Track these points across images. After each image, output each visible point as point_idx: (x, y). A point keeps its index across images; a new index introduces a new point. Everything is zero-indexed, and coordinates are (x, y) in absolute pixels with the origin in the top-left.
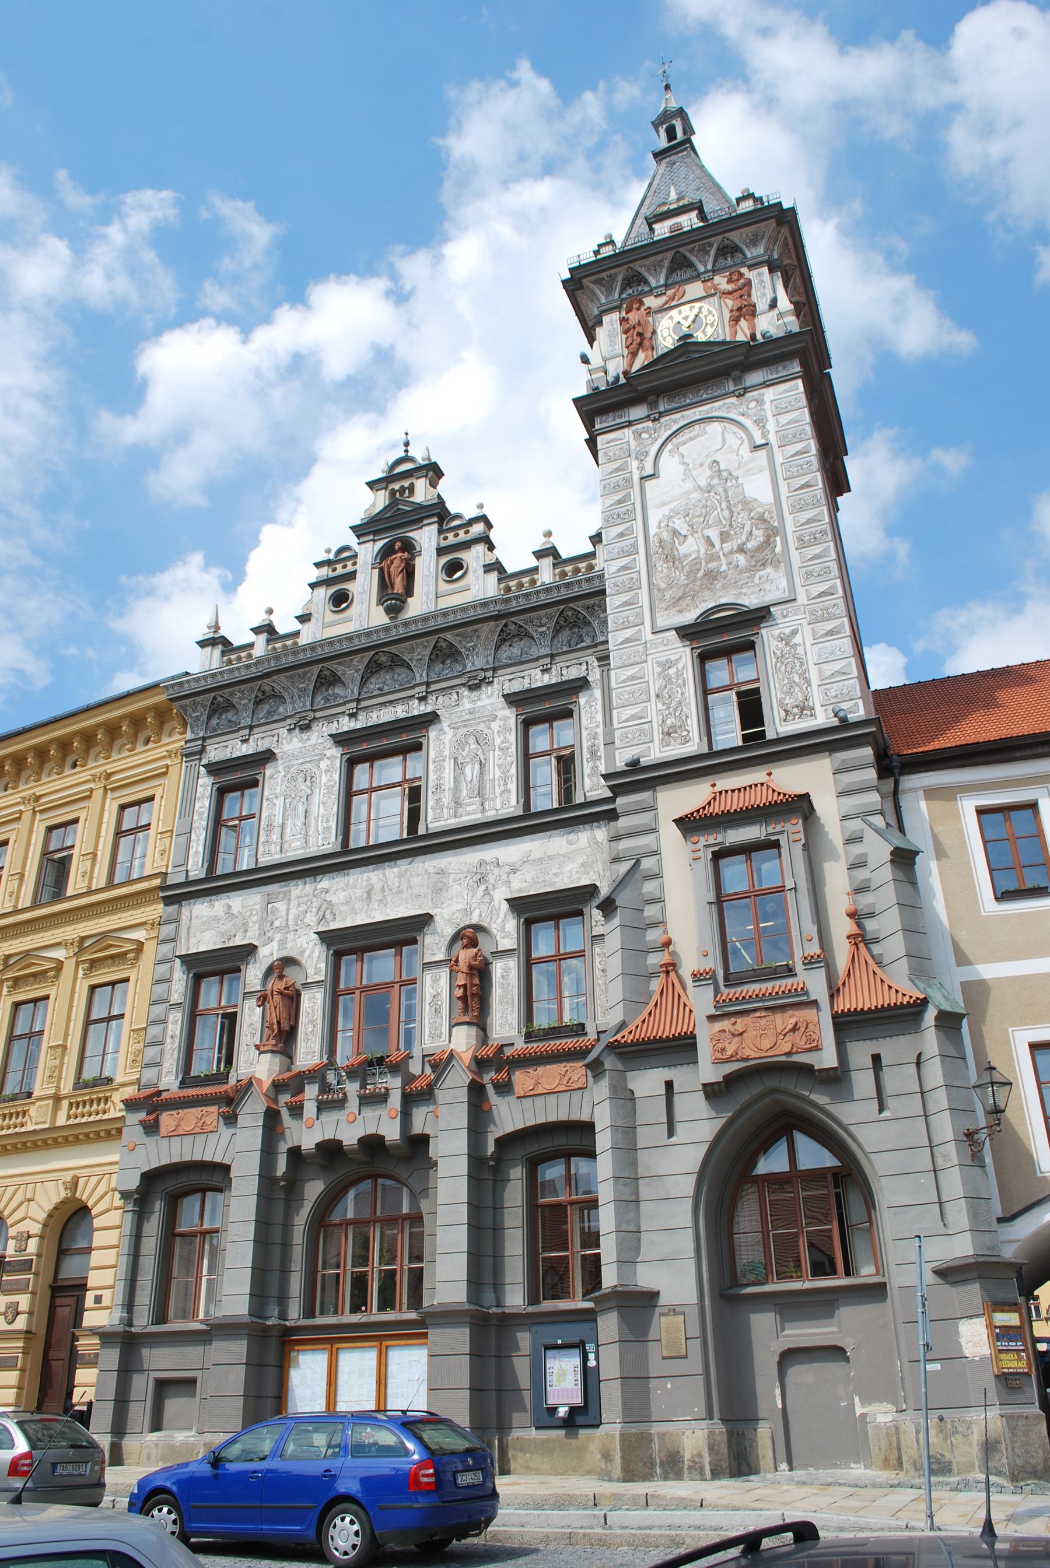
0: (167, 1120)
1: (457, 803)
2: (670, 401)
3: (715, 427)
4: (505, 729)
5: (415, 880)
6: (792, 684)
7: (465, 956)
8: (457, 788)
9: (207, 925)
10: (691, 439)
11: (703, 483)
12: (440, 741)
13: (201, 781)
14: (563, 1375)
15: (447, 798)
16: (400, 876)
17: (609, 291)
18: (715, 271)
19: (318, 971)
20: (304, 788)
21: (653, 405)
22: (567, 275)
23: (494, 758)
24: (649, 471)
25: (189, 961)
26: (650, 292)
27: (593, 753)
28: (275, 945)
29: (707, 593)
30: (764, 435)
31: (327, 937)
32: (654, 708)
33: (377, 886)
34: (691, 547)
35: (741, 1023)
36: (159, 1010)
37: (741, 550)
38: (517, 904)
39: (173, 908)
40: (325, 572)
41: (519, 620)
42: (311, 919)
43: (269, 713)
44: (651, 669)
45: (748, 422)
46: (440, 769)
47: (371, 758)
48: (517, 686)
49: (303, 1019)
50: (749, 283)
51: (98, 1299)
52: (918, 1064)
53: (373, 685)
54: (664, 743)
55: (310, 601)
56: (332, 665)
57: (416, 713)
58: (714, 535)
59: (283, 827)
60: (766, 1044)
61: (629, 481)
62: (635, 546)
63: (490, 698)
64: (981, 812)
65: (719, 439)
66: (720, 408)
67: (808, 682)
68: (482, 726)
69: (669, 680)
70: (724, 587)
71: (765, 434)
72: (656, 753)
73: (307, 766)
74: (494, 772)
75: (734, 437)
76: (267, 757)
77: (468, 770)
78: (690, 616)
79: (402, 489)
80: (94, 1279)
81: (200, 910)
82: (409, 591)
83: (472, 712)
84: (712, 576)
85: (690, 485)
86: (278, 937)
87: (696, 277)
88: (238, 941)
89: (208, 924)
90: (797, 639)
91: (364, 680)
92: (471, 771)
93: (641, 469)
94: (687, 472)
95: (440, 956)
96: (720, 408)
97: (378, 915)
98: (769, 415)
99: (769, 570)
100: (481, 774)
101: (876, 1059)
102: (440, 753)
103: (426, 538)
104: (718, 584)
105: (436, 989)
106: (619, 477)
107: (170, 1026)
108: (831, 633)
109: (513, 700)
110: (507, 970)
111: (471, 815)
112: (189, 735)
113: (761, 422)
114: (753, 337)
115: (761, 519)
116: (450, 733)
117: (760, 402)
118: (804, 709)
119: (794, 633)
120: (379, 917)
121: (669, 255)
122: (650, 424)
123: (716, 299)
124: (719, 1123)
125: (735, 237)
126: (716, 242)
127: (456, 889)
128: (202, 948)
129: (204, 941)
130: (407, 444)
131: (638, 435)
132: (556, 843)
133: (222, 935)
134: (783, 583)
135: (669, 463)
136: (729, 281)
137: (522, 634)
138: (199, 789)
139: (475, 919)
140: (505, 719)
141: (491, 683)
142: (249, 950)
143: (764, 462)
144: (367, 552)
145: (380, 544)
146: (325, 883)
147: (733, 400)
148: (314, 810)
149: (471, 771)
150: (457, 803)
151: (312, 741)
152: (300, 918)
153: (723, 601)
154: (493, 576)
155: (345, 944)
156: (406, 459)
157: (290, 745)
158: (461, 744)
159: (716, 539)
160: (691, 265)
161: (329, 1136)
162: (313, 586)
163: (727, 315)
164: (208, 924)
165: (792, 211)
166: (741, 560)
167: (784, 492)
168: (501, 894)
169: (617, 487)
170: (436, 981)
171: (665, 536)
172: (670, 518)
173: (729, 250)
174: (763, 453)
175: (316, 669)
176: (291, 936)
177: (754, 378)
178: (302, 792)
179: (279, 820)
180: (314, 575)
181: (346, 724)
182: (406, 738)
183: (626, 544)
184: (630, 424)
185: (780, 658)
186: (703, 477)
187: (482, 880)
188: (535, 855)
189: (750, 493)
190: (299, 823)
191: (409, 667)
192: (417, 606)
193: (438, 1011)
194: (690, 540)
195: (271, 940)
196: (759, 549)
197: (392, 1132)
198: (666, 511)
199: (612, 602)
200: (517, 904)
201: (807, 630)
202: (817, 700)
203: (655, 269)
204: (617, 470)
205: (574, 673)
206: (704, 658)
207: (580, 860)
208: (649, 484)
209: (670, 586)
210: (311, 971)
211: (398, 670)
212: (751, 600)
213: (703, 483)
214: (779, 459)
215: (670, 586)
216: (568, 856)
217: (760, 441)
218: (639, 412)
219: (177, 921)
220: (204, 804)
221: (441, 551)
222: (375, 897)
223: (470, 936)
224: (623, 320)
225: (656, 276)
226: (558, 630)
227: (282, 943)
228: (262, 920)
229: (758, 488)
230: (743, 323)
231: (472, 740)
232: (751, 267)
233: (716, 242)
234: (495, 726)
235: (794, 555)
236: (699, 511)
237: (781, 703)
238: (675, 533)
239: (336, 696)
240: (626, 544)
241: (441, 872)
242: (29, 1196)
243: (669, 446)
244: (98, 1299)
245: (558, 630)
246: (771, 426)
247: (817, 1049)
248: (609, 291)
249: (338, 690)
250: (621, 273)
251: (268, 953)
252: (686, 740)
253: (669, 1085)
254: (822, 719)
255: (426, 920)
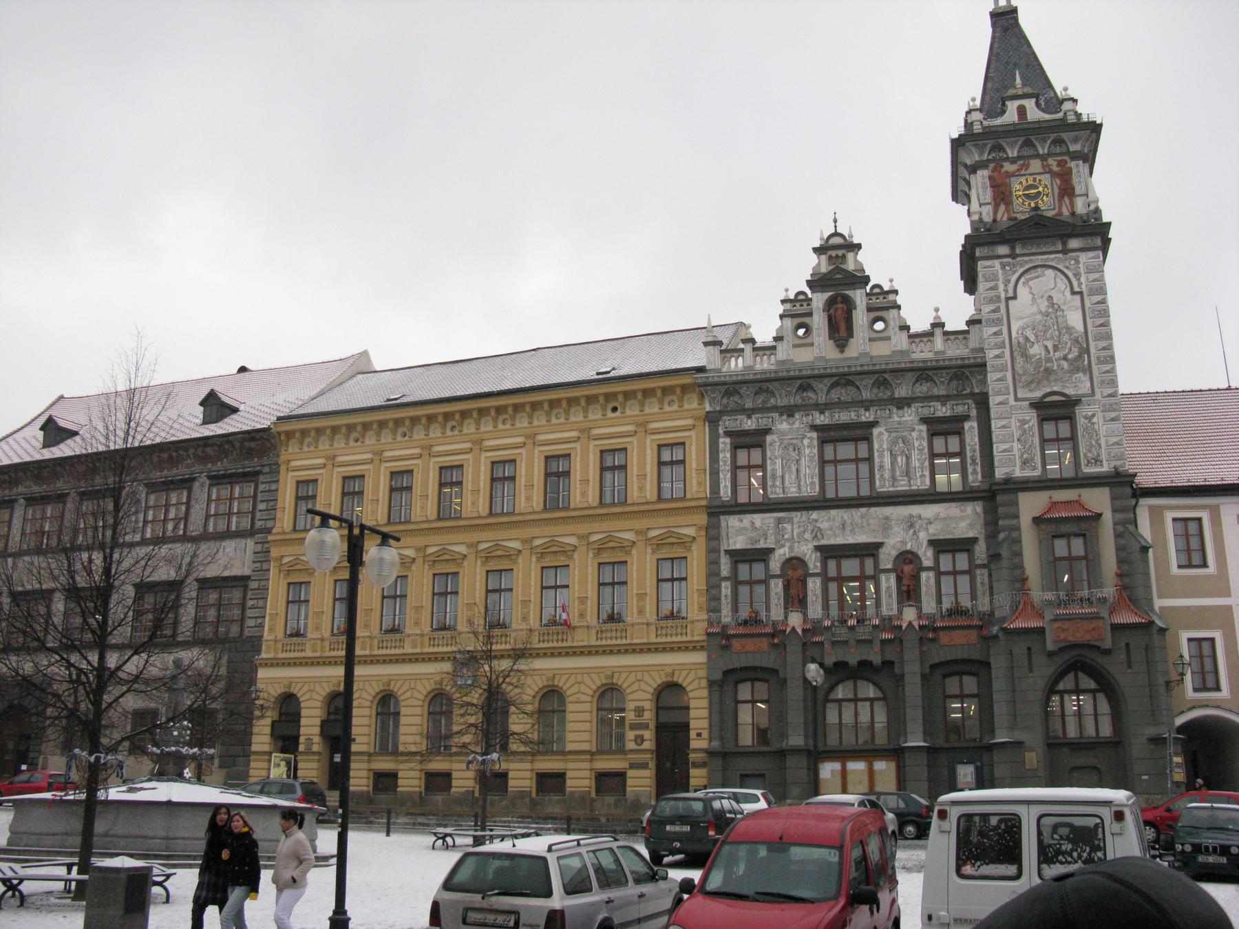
0: (736, 644)
1: (894, 478)
2: (1023, 247)
3: (1050, 272)
4: (920, 438)
5: (871, 521)
6: (1091, 446)
7: (908, 569)
8: (893, 470)
9: (739, 532)
10: (1036, 277)
11: (1043, 310)
12: (881, 438)
13: (721, 440)
14: (965, 775)
15: (887, 475)
16: (862, 517)
17: (982, 153)
18: (1050, 155)
19: (816, 567)
20: (794, 455)
21: (1013, 248)
22: (956, 136)
23: (915, 455)
24: (1011, 294)
25: (732, 553)
26: (1007, 159)
27: (974, 461)
28: (786, 549)
29: (1045, 382)
30: (1080, 284)
31: (817, 548)
32: (1016, 446)
33: (849, 522)
34: (1036, 350)
35: (1066, 625)
36: (713, 580)
37: (1065, 358)
38: (932, 543)
39: (713, 520)
40: (788, 306)
41: (930, 373)
42: (807, 536)
43: (764, 402)
44: (1014, 423)
45: (1070, 274)
46: (881, 456)
47: (834, 441)
48: (926, 412)
49: (809, 593)
50: (1070, 171)
51: (699, 735)
52: (1146, 648)
53: (834, 395)
54: (1022, 468)
55: (781, 327)
56: (812, 382)
57: (863, 419)
58: (1050, 345)
59: (783, 477)
60: (1079, 635)
61: (999, 297)
62: (1003, 342)
63: (909, 416)
64: (1174, 520)
65: (1052, 281)
66: (1052, 260)
67: (1100, 446)
68: (905, 434)
69: (1025, 431)
70: (1055, 380)
71: (1080, 284)
72: (1018, 473)
73: (795, 441)
74: (915, 463)
75: (1062, 284)
76: (767, 431)
77: (899, 459)
78: (1038, 394)
79: (837, 256)
80: (693, 724)
81: (732, 523)
82: (851, 335)
83: (899, 423)
84: (1048, 371)
85: (1035, 309)
86: (788, 544)
87: (1037, 156)
88: (762, 545)
89: (741, 531)
90: (1095, 420)
91: (828, 392)
92: (901, 460)
93: (1006, 291)
94: (1034, 299)
95: (889, 566)
96: (1052, 260)
97: (851, 540)
98: (1082, 271)
99: (1081, 374)
100: (908, 463)
101: (1127, 645)
102: (881, 446)
103: (859, 297)
104: (1052, 378)
105: (889, 582)
106: (993, 293)
107: (724, 591)
108: (1113, 420)
109: (924, 420)
110: (928, 578)
111: (902, 486)
112: (708, 408)
113: (1077, 275)
114: (1073, 214)
115: (1077, 341)
116: (886, 435)
117: (1077, 262)
118: (1097, 461)
119: (1093, 416)
120: (851, 540)
121: (1023, 139)
122: (1009, 260)
123: (1048, 176)
124: (1053, 670)
125: (1065, 136)
126: (1053, 136)
127: (896, 529)
128: (738, 547)
129: (739, 543)
130: (835, 221)
131: (1003, 266)
132: (952, 509)
133: (751, 539)
134: (1089, 385)
135: (1022, 291)
136: (1058, 165)
137: (929, 379)
138: (721, 446)
139: (909, 547)
140: (921, 431)
141: (909, 406)
142: (770, 551)
143: (1078, 303)
144: (819, 300)
145: (827, 295)
146: (815, 515)
147: (1060, 255)
148: (803, 469)
149: (901, 460)
150: (894, 478)
151: (797, 425)
152: (801, 535)
153: (1055, 389)
154: (904, 335)
155: (829, 553)
156: (836, 234)
157: (782, 425)
158: (895, 443)
159: (1050, 348)
160: (1034, 146)
161: (840, 658)
162: (782, 317)
163: (1056, 191)
164: (741, 531)
165: (1101, 125)
166: (1065, 365)
167: (1090, 328)
168: (923, 537)
169: (991, 301)
170: (888, 579)
171: (1021, 340)
172: (1024, 328)
173: (1059, 142)
174: (1078, 297)
175: (799, 382)
176: (796, 545)
177: (1074, 243)
178: (792, 460)
179: (779, 473)
180: (780, 309)
181: (821, 419)
182: (861, 433)
183: (998, 339)
184: (999, 257)
185: (1085, 429)
186: (1044, 305)
187: (912, 526)
188: (942, 515)
189: (1071, 323)
190: (794, 477)
191: (858, 388)
192: (859, 346)
193: (890, 596)
194: (1036, 346)
195: (783, 546)
196: (1075, 359)
197: (876, 659)
198: (1021, 323)
199: (992, 376)
200: (932, 543)
201: (1100, 415)
202: (1104, 457)
203: (1012, 145)
204: (991, 289)
205: (960, 410)
206: (1042, 420)
207: (968, 521)
208: (1011, 303)
209: (1024, 374)
210: (811, 566)
211: (849, 388)
212: (1070, 391)
213: (1043, 310)
214: (1087, 304)
215: (1024, 374)
216: (962, 519)
217: (1076, 289)
218: (1003, 250)
219: (718, 527)
220: (725, 456)
221: (869, 309)
222: (848, 528)
223: (907, 557)
224: (990, 178)
225: (1012, 148)
226: (951, 379)
227: (791, 548)
228: (776, 534)
229: (1074, 319)
230: (1066, 200)
231: (900, 441)
232: (1073, 159)
233: (1053, 136)
234: (914, 434)
235: (1094, 367)
236: (1041, 328)
237: (1085, 456)
238: (1027, 339)
239: (809, 398)
240: (998, 339)
241: (887, 518)
242: (639, 677)
243: (1023, 280)
244: (699, 735)
245: (951, 379)
246: (1083, 279)
247: (1102, 640)
248: (982, 153)
249: (811, 395)
250: (990, 143)
251: (782, 553)
252: (1034, 468)
253: (1029, 649)
254: (1105, 468)
255: (879, 545)
